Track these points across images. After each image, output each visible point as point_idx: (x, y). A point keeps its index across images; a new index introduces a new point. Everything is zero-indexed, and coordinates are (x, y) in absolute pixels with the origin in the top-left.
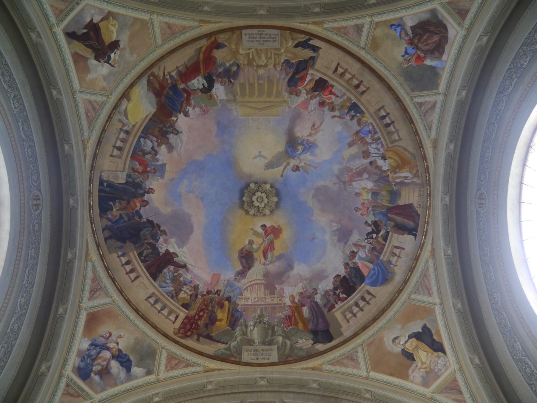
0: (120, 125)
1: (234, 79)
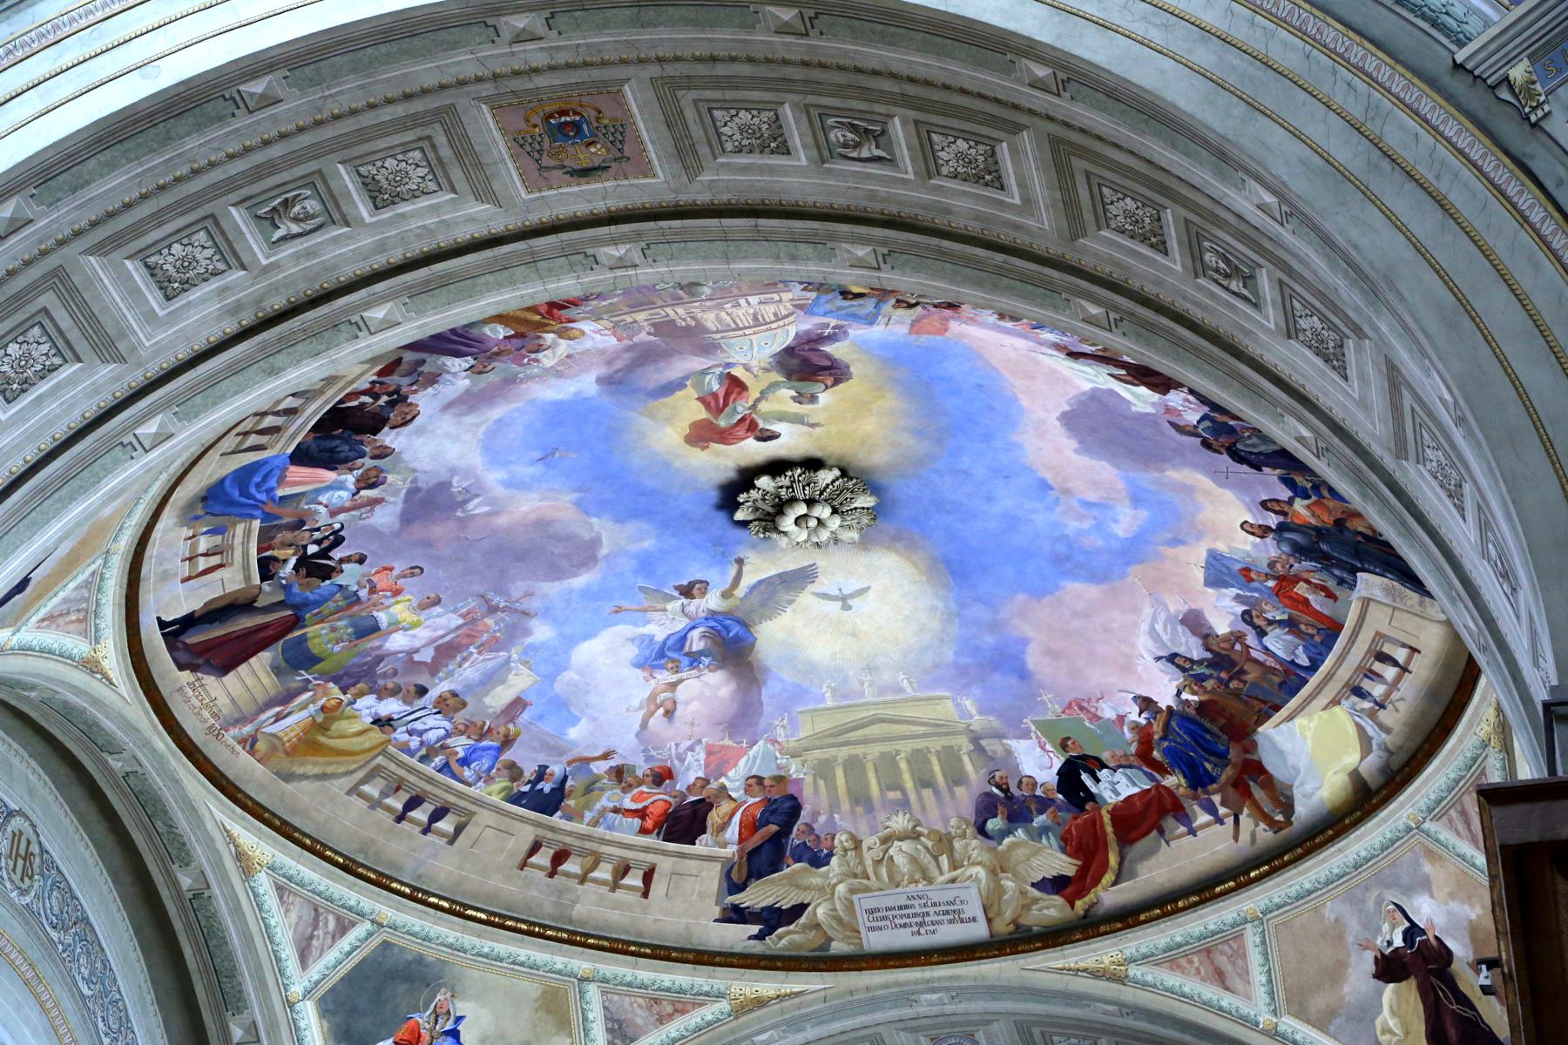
0: (1384, 716)
1: (989, 795)
